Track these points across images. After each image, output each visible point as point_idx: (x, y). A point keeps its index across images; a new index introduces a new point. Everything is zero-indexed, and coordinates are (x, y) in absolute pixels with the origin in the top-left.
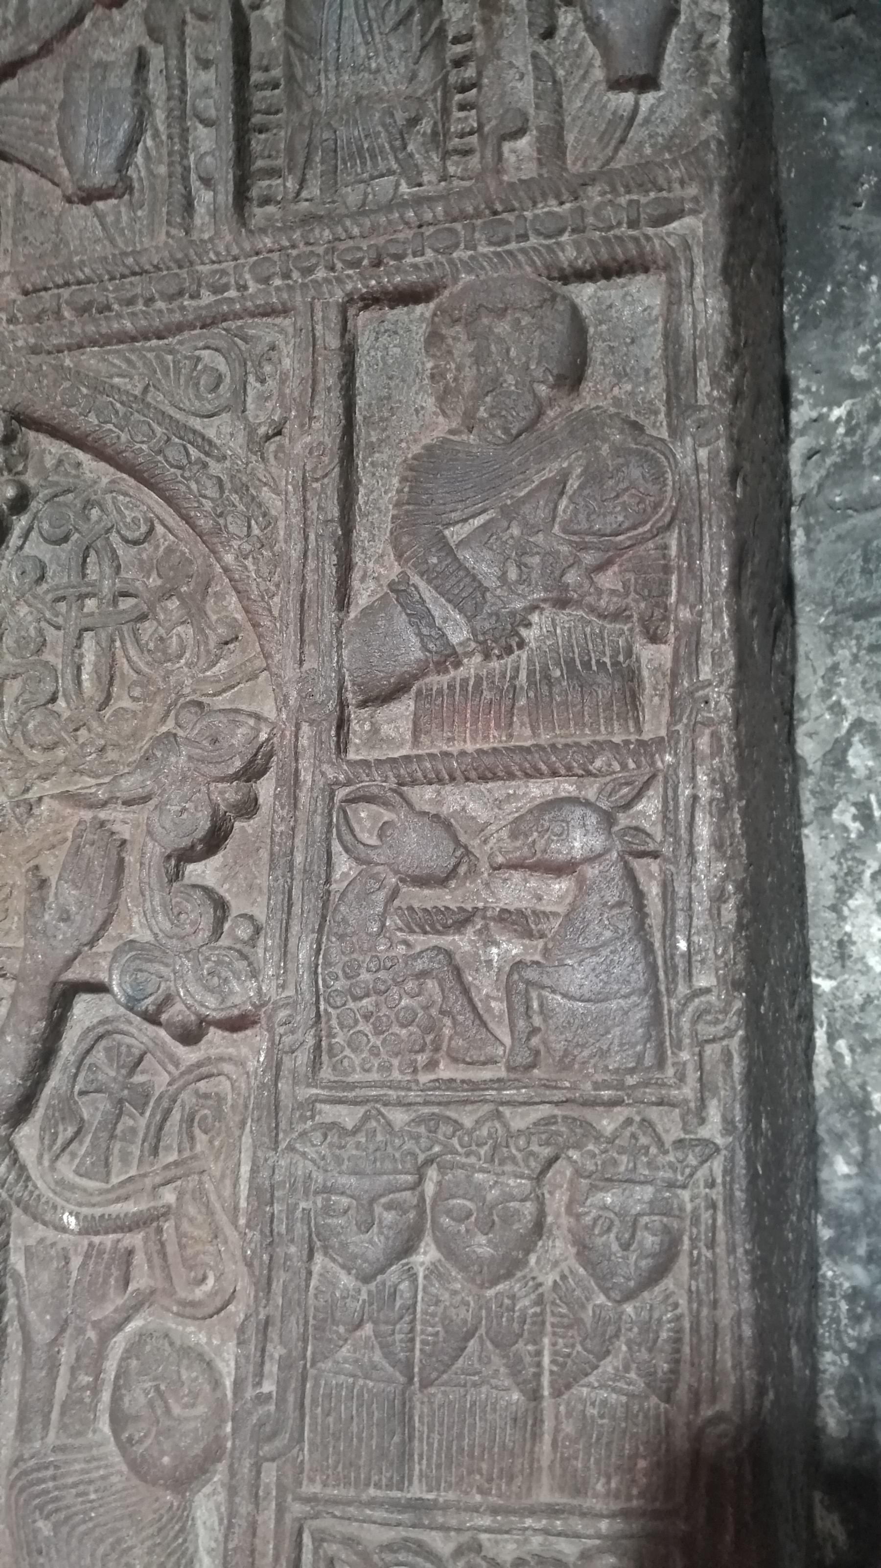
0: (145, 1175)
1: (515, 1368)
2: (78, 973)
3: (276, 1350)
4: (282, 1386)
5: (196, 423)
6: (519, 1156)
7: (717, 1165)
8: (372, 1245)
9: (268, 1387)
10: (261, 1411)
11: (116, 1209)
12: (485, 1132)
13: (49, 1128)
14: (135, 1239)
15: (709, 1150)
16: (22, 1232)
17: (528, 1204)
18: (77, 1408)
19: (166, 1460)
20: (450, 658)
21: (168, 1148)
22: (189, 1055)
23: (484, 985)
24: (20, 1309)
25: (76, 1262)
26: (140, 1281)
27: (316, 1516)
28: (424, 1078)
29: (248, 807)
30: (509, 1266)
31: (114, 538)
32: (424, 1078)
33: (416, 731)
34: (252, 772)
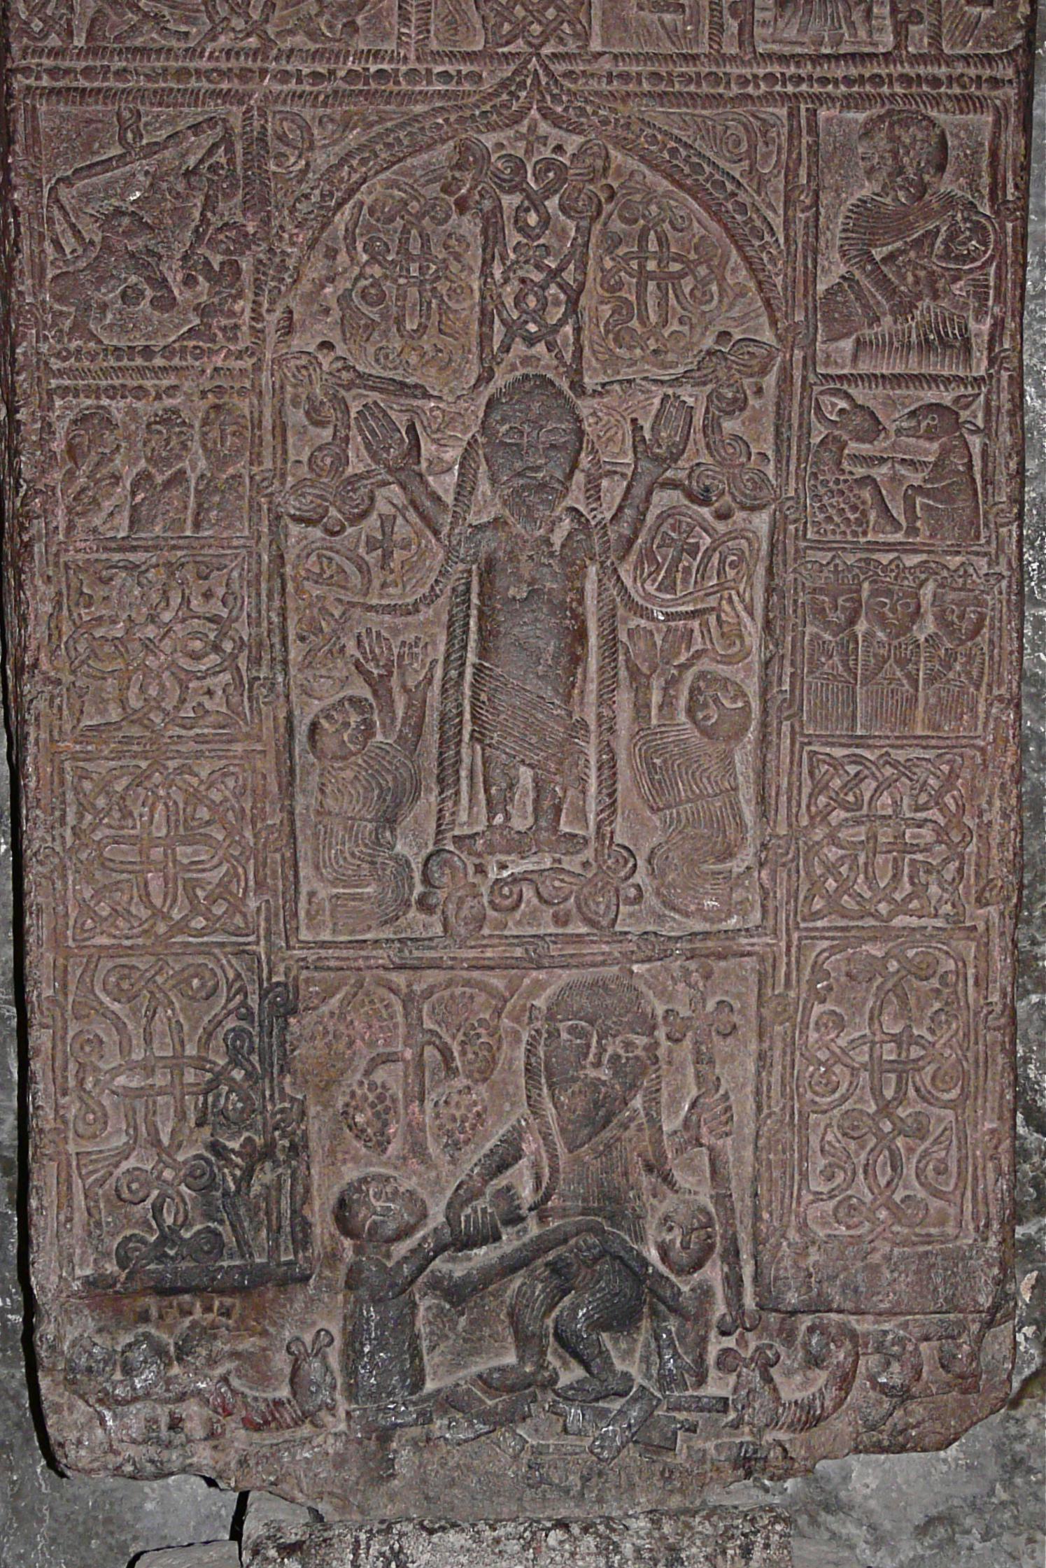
1: (908, 675)
3: (788, 670)
4: (792, 684)
7: (1004, 583)
8: (837, 617)
9: (786, 687)
11: (680, 609)
13: (639, 564)
14: (696, 624)
16: (625, 621)
18: (667, 704)
21: (710, 578)
22: (721, 527)
24: (627, 661)
26: (698, 645)
27: (810, 744)
33: (855, 358)
34: (764, 371)
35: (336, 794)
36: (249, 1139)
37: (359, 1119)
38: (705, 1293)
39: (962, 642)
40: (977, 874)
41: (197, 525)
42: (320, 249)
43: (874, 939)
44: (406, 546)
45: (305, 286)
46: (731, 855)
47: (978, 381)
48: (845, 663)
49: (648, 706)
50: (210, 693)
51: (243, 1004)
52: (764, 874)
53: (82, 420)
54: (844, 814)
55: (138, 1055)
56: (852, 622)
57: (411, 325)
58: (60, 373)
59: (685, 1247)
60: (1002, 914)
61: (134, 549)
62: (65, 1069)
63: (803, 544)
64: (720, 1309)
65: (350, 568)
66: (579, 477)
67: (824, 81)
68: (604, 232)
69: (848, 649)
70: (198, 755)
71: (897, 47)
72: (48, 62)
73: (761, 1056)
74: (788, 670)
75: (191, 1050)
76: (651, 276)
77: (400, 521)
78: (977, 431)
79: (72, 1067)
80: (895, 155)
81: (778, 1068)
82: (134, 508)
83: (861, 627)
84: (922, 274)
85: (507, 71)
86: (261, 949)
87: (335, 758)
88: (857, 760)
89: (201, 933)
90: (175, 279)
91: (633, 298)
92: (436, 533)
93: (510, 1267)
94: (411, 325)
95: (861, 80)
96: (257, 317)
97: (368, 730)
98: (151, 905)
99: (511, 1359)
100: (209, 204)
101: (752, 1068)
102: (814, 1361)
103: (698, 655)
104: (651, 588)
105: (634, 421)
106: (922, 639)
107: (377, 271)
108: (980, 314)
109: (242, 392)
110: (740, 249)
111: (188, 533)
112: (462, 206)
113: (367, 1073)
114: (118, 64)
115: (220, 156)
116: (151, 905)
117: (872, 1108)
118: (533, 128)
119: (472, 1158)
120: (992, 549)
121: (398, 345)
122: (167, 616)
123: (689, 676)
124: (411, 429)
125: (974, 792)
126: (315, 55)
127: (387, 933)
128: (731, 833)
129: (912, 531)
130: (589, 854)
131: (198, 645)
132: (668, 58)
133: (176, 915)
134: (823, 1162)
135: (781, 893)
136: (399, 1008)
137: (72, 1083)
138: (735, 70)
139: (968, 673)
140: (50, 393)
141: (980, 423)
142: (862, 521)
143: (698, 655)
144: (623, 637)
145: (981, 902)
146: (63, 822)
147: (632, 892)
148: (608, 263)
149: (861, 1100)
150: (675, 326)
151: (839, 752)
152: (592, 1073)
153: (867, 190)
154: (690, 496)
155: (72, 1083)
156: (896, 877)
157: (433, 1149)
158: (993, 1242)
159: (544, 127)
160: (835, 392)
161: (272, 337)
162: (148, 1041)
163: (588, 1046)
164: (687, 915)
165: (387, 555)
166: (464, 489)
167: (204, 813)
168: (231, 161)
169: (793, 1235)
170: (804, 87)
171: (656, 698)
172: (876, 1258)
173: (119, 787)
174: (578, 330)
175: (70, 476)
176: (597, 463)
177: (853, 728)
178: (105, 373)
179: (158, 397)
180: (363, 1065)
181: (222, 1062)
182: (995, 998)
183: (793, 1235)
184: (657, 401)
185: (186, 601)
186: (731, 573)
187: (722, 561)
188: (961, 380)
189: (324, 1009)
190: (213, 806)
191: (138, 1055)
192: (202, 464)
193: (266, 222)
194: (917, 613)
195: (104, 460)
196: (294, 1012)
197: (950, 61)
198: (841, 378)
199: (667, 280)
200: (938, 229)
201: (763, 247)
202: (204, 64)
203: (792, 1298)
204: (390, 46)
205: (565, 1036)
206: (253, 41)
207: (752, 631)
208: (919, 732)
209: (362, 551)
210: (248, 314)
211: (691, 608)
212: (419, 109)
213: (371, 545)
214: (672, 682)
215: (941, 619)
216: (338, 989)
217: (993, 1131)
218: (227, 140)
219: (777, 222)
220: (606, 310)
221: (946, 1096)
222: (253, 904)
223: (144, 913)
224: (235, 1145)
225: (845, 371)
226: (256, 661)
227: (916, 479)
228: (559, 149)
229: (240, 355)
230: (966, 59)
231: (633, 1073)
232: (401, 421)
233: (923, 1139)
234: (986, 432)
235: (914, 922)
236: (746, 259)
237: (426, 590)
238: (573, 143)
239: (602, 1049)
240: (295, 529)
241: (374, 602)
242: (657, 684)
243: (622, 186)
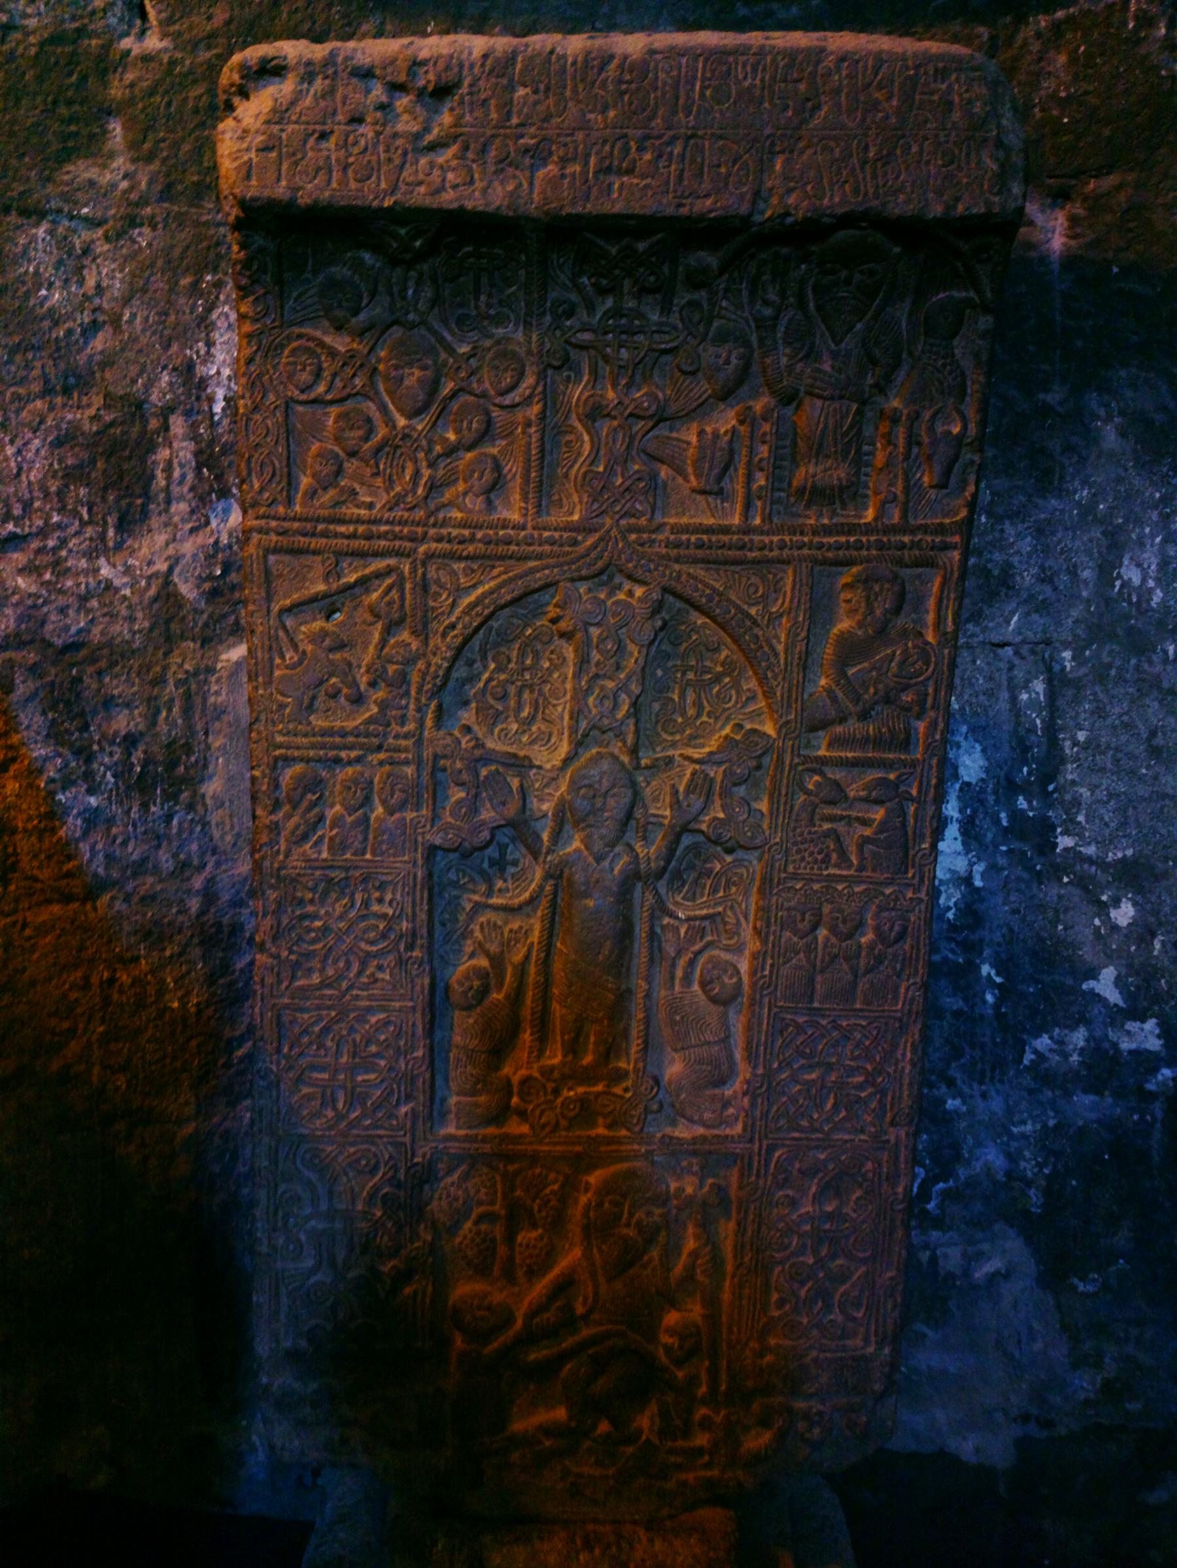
1: (851, 968)
2: (693, 826)
3: (769, 962)
4: (771, 972)
5: (745, 607)
7: (923, 907)
8: (804, 926)
9: (767, 972)
11: (698, 912)
13: (670, 882)
14: (707, 923)
15: (921, 900)
18: (687, 979)
20: (842, 720)
22: (729, 859)
23: (847, 841)
25: (683, 931)
29: (759, 767)
30: (850, 936)
31: (702, 648)
33: (830, 745)
35: (462, 1029)
36: (394, 1267)
37: (470, 1253)
38: (693, 1381)
40: (892, 1105)
41: (374, 854)
42: (461, 662)
43: (817, 1147)
44: (515, 863)
45: (451, 684)
46: (724, 1083)
47: (913, 764)
48: (808, 959)
49: (672, 978)
50: (380, 968)
51: (393, 1177)
52: (746, 1100)
53: (298, 779)
54: (802, 1061)
55: (324, 1207)
56: (814, 928)
57: (525, 714)
58: (280, 746)
59: (681, 1347)
60: (907, 1134)
61: (332, 867)
62: (276, 1214)
64: (704, 1389)
65: (477, 878)
66: (633, 823)
67: (820, 546)
68: (658, 651)
69: (810, 949)
70: (369, 1010)
71: (876, 519)
72: (273, 524)
73: (739, 1224)
74: (769, 962)
75: (359, 1207)
76: (689, 683)
77: (511, 847)
78: (912, 799)
79: (280, 1214)
80: (868, 598)
81: (749, 1233)
82: (331, 839)
83: (822, 933)
84: (880, 686)
85: (597, 535)
86: (407, 1139)
87: (463, 1009)
88: (814, 1024)
89: (367, 1128)
90: (363, 681)
91: (676, 698)
92: (536, 859)
93: (563, 1357)
94: (525, 714)
95: (848, 546)
96: (419, 710)
97: (484, 992)
98: (334, 1108)
99: (561, 1413)
100: (388, 631)
101: (732, 1225)
102: (765, 1423)
103: (709, 945)
104: (679, 898)
105: (673, 786)
106: (863, 940)
107: (503, 677)
108: (919, 717)
109: (407, 762)
110: (752, 666)
111: (368, 856)
112: (563, 635)
113: (476, 1223)
114: (320, 527)
115: (394, 594)
116: (334, 1108)
117: (811, 1261)
118: (611, 578)
119: (542, 1285)
120: (916, 881)
121: (515, 727)
122: (352, 914)
123: (702, 960)
124: (521, 786)
125: (894, 1046)
126: (463, 525)
127: (491, 1130)
128: (725, 1067)
129: (861, 868)
130: (629, 1083)
131: (372, 935)
132: (709, 530)
133: (353, 1116)
134: (775, 1297)
135: (758, 1113)
136: (498, 1178)
137: (280, 1224)
138: (756, 538)
139: (894, 968)
140: (276, 759)
141: (914, 792)
142: (826, 861)
143: (709, 945)
144: (658, 930)
145: (893, 1123)
146: (278, 1050)
147: (655, 1107)
148: (659, 673)
149: (803, 1254)
150: (705, 718)
151: (801, 1020)
152: (625, 1231)
153: (844, 624)
154: (709, 840)
155: (280, 1224)
156: (835, 1105)
157: (520, 1273)
158: (887, 1351)
159: (618, 579)
160: (813, 771)
161: (429, 723)
162: (330, 1200)
163: (622, 1213)
164: (691, 1120)
165: (502, 870)
166: (556, 836)
167: (373, 1049)
168: (402, 598)
169: (753, 1344)
170: (805, 551)
171: (679, 973)
172: (808, 1360)
173: (317, 1029)
174: (636, 724)
175: (289, 817)
176: (646, 815)
178: (313, 746)
179: (350, 763)
180: (474, 1216)
181: (379, 1214)
182: (900, 1190)
183: (753, 1344)
184: (688, 772)
185: (366, 904)
186: (734, 889)
187: (728, 881)
188: (904, 763)
189: (449, 1180)
190: (379, 1043)
191: (324, 1207)
192: (380, 810)
193: (426, 642)
194: (861, 924)
195: (314, 804)
196: (427, 1182)
197: (913, 531)
198: (818, 759)
199: (701, 686)
200: (894, 652)
201: (768, 668)
202: (383, 528)
203: (750, 1384)
204: (515, 517)
205: (607, 1205)
206: (420, 514)
207: (747, 932)
208: (858, 1006)
209: (486, 865)
210: (412, 706)
211: (705, 912)
212: (532, 564)
213: (492, 863)
214: (692, 963)
215: (877, 929)
216: (458, 1166)
217: (892, 1278)
218: (400, 584)
219: (780, 648)
220: (656, 706)
221: (861, 1255)
222: (404, 1109)
223: (330, 1113)
224: (386, 1269)
225: (822, 752)
226: (410, 947)
227: (868, 832)
228: (630, 593)
229: (406, 736)
230: (925, 529)
231: (649, 1236)
232: (515, 783)
233: (843, 1283)
234: (919, 801)
235: (846, 1137)
236: (756, 673)
237: (527, 895)
238: (639, 592)
239: (631, 1215)
240: (440, 853)
241: (494, 901)
242: (682, 963)
243: (672, 619)
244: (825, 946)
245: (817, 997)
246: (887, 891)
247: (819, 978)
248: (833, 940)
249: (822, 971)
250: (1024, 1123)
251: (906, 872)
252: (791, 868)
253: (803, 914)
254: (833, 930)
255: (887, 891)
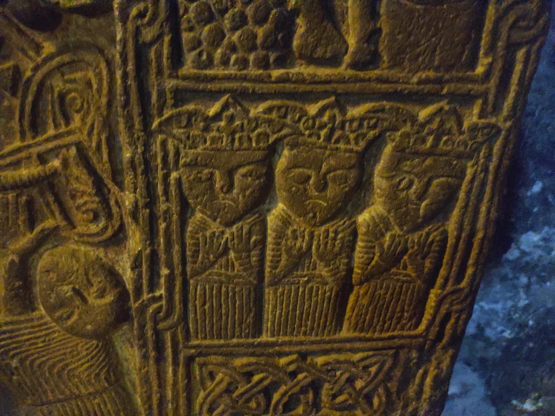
0: (29, 146)
6: (352, 136)
9: (161, 292)
10: (155, 306)
12: (325, 118)
17: (352, 171)
19: (89, 327)
28: (276, 73)
32: (276, 73)
39: (417, 228)
63: (170, 84)
177: (258, 330)
215: (392, 196)
244: (280, 235)
245: (268, 325)
246: (424, 114)
247: (269, 293)
248: (299, 224)
249: (275, 283)
250: (496, 302)
251: (473, 63)
252: (188, 69)
253: (230, 174)
254: (298, 201)
255: (424, 114)
